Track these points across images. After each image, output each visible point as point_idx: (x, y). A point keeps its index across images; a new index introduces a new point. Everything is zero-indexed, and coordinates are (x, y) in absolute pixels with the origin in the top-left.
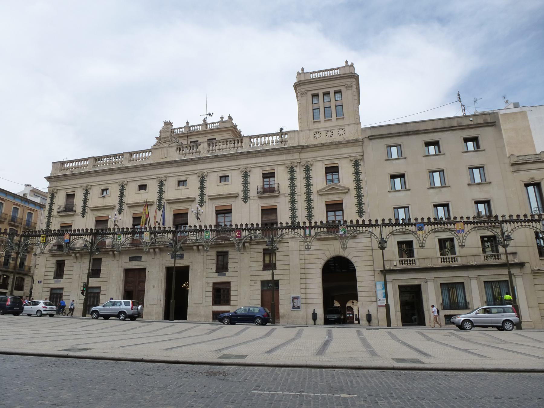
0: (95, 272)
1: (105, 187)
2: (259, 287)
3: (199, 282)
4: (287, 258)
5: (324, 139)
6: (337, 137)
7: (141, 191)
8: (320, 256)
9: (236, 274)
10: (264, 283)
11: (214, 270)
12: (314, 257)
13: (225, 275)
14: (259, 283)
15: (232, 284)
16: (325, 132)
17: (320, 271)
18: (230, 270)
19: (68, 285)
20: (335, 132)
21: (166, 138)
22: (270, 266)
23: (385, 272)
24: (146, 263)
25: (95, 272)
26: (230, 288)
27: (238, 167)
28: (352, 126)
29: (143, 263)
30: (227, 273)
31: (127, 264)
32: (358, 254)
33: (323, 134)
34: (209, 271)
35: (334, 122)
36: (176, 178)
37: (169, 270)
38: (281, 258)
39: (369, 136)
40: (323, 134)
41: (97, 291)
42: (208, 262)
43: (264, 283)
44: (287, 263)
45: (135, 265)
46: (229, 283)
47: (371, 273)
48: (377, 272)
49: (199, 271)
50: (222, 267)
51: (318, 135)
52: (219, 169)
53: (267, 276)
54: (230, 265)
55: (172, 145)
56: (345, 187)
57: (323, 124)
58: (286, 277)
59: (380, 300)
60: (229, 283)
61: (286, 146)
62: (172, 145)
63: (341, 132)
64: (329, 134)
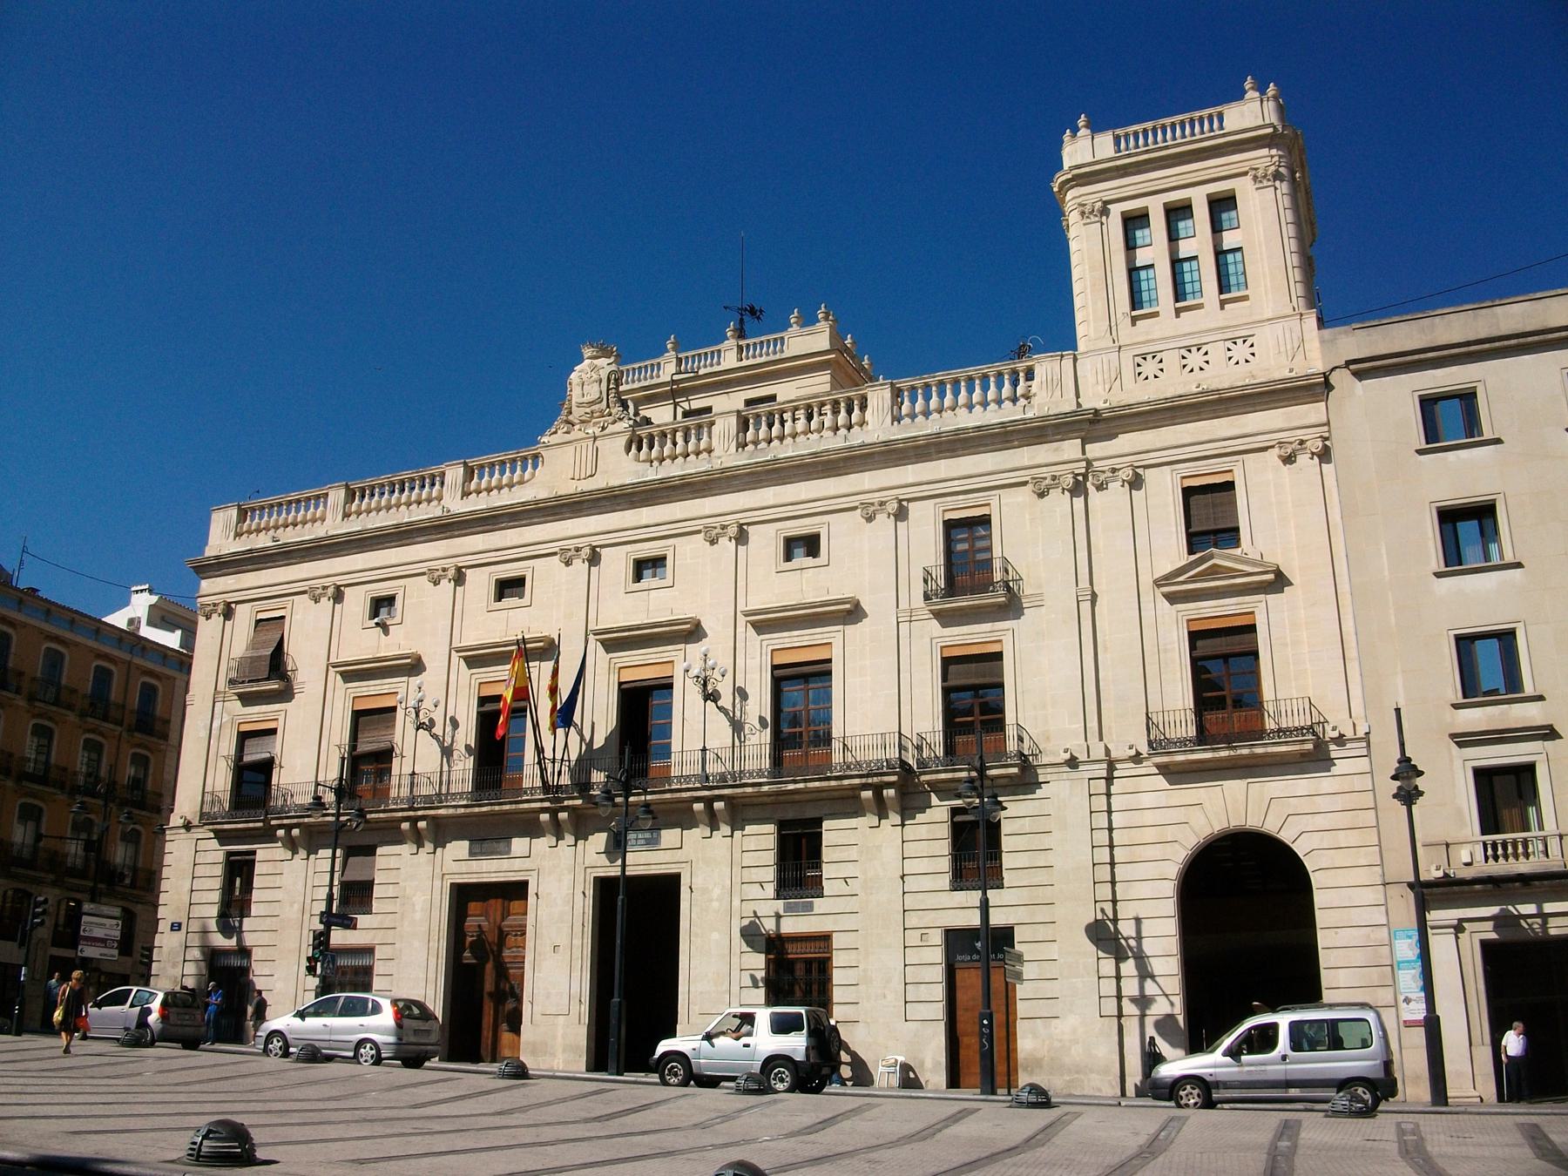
1: (383, 589)
3: (715, 936)
4: (1045, 841)
5: (1174, 384)
6: (1222, 375)
7: (506, 602)
8: (1169, 833)
9: (851, 904)
10: (956, 940)
11: (770, 890)
12: (1149, 835)
13: (810, 907)
14: (937, 938)
15: (837, 941)
16: (1176, 354)
17: (1169, 889)
20: (1217, 352)
23: (1430, 894)
24: (526, 864)
26: (830, 959)
29: (517, 864)
30: (815, 900)
31: (464, 867)
32: (1320, 822)
33: (1171, 359)
34: (755, 891)
36: (628, 548)
37: (605, 887)
39: (1348, 363)
40: (1171, 359)
42: (749, 859)
43: (956, 940)
44: (1041, 860)
45: (490, 870)
46: (826, 938)
49: (716, 892)
51: (1150, 367)
53: (963, 910)
56: (1260, 563)
57: (1165, 325)
59: (1407, 1000)
60: (826, 938)
61: (1029, 415)
62: (611, 429)
63: (1240, 351)
64: (1195, 359)
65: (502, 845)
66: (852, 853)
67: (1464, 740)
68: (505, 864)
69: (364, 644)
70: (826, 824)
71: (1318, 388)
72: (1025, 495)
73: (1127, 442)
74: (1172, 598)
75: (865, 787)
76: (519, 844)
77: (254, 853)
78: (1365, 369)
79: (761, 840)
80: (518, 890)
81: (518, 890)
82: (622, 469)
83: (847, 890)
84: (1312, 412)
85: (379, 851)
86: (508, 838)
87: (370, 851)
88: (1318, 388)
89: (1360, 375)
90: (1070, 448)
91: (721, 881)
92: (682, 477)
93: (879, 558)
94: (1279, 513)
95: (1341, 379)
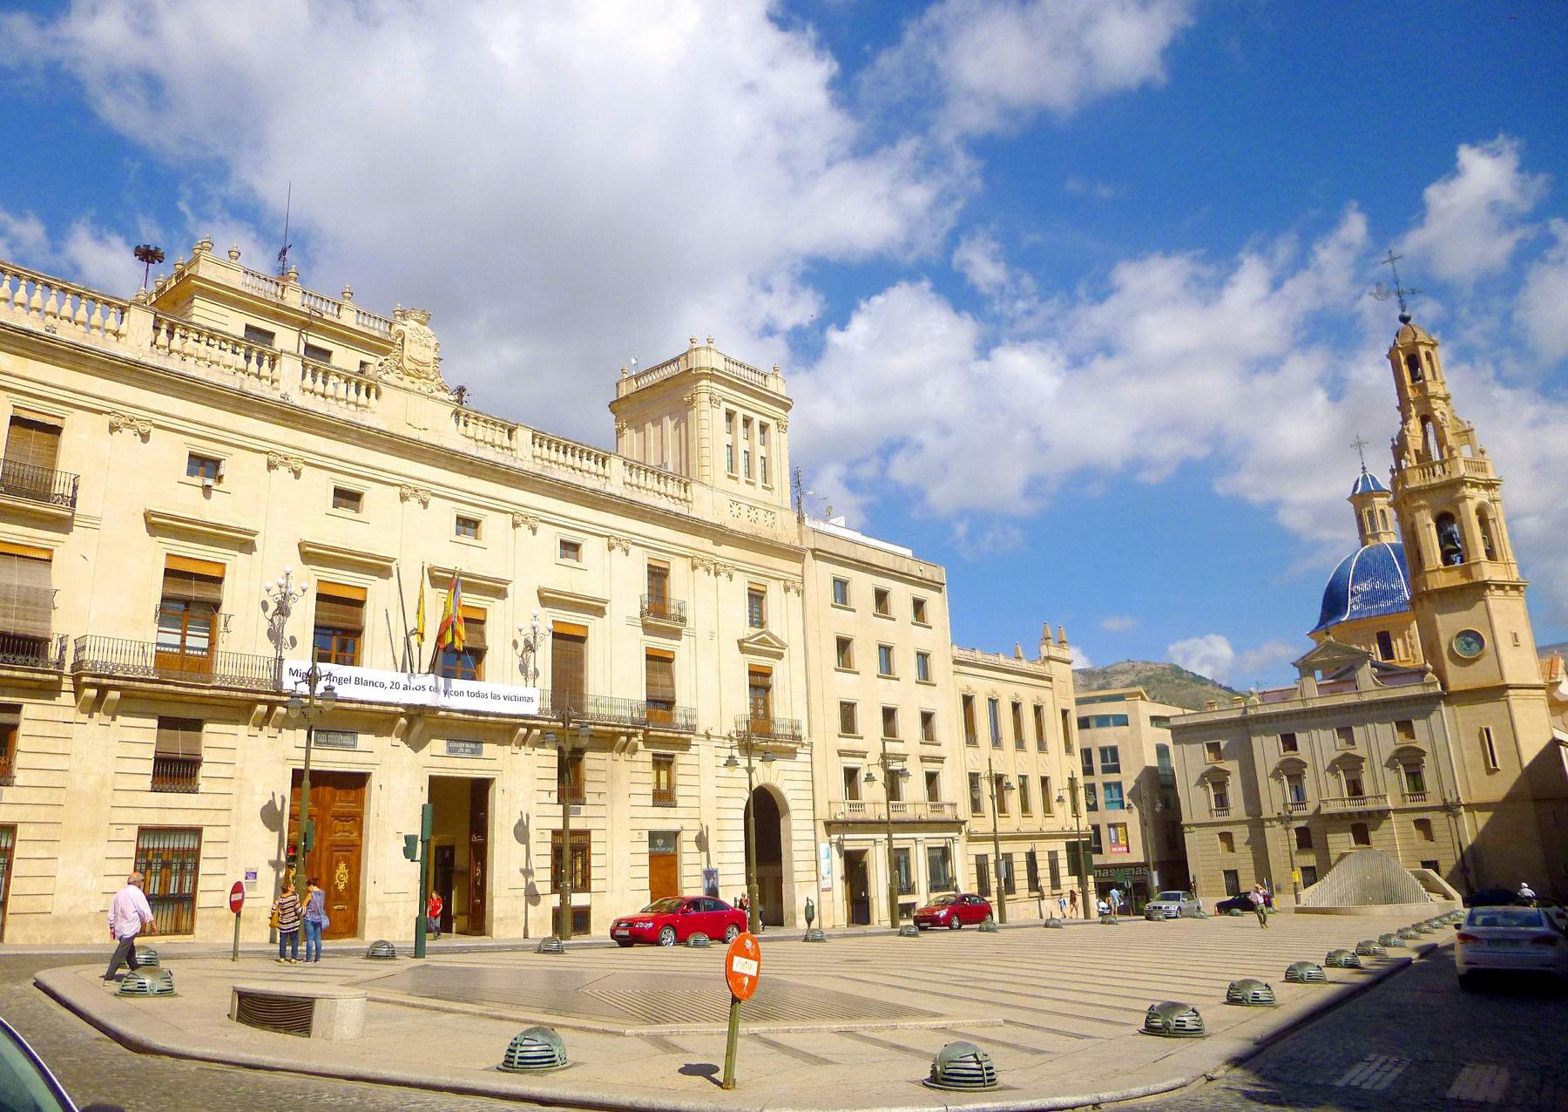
0: (175, 771)
1: (208, 449)
2: (645, 848)
14: (646, 837)
15: (594, 836)
18: (589, 799)
19: (42, 814)
21: (424, 364)
22: (664, 797)
25: (175, 771)
27: (608, 532)
28: (784, 513)
35: (757, 493)
38: (139, 751)
41: (188, 843)
43: (653, 836)
46: (587, 833)
47: (810, 825)
48: (820, 825)
50: (570, 786)
52: (561, 521)
54: (588, 787)
55: (436, 394)
57: (742, 488)
58: (222, 818)
60: (587, 833)
62: (436, 394)
65: (347, 739)
66: (602, 777)
67: (841, 753)
68: (349, 756)
69: (186, 501)
70: (588, 755)
71: (795, 554)
72: (686, 563)
73: (726, 550)
74: (743, 650)
75: (622, 734)
76: (364, 740)
77: (16, 709)
78: (818, 554)
79: (547, 759)
80: (356, 782)
81: (356, 782)
82: (450, 435)
83: (599, 801)
84: (795, 567)
85: (207, 727)
86: (354, 733)
87: (196, 725)
88: (795, 554)
89: (815, 557)
90: (707, 544)
91: (521, 784)
92: (509, 468)
93: (616, 578)
94: (781, 613)
95: (809, 555)
